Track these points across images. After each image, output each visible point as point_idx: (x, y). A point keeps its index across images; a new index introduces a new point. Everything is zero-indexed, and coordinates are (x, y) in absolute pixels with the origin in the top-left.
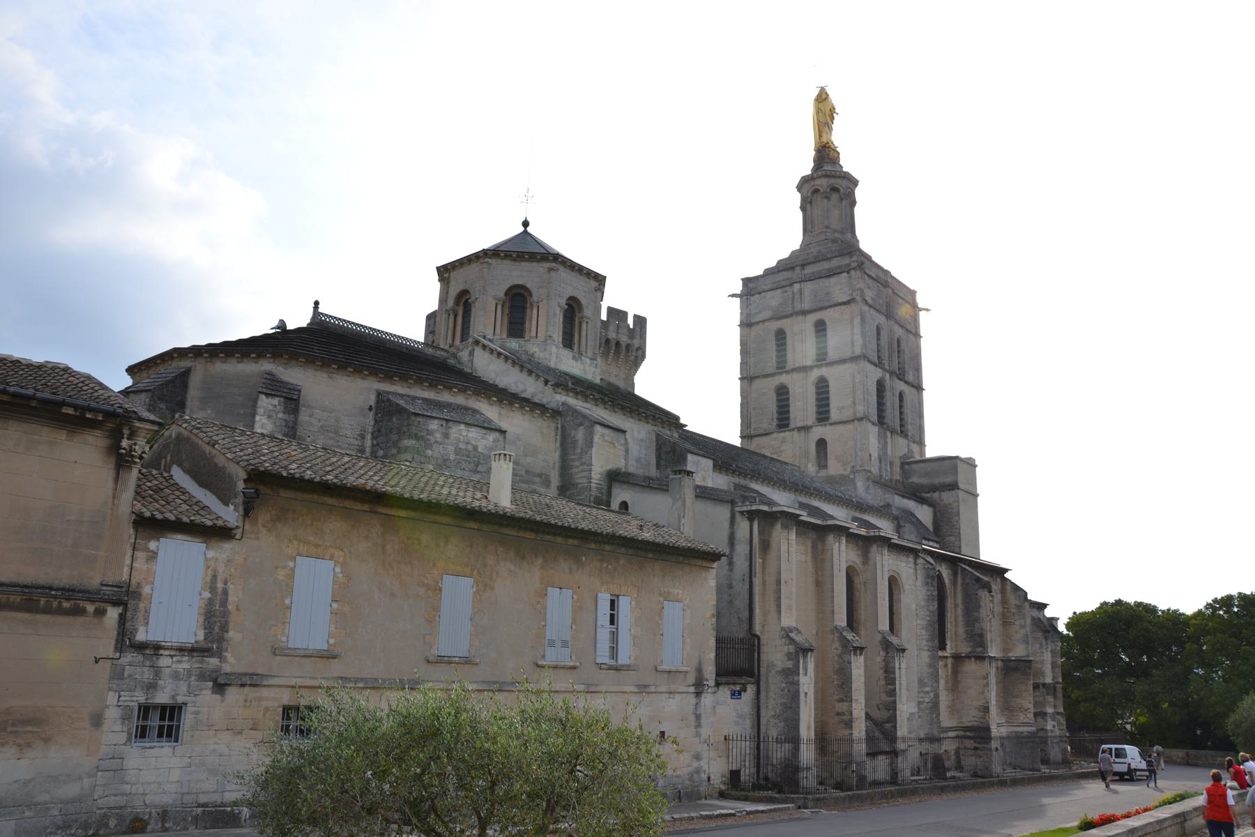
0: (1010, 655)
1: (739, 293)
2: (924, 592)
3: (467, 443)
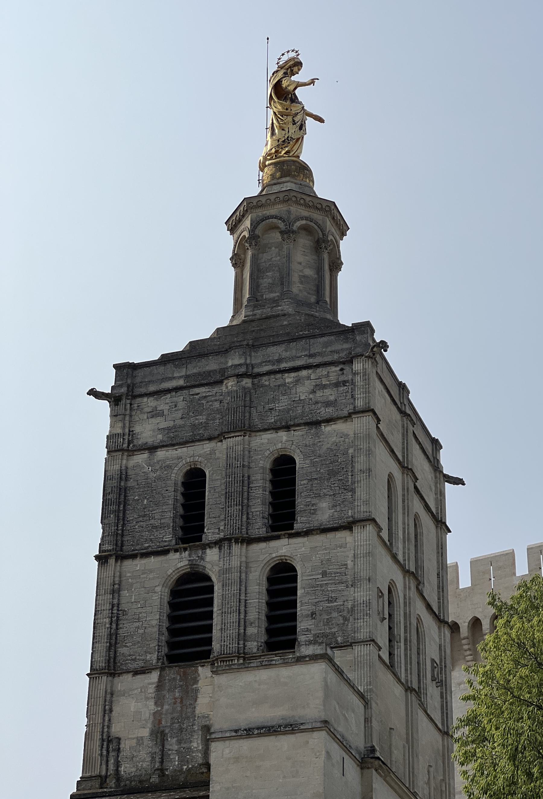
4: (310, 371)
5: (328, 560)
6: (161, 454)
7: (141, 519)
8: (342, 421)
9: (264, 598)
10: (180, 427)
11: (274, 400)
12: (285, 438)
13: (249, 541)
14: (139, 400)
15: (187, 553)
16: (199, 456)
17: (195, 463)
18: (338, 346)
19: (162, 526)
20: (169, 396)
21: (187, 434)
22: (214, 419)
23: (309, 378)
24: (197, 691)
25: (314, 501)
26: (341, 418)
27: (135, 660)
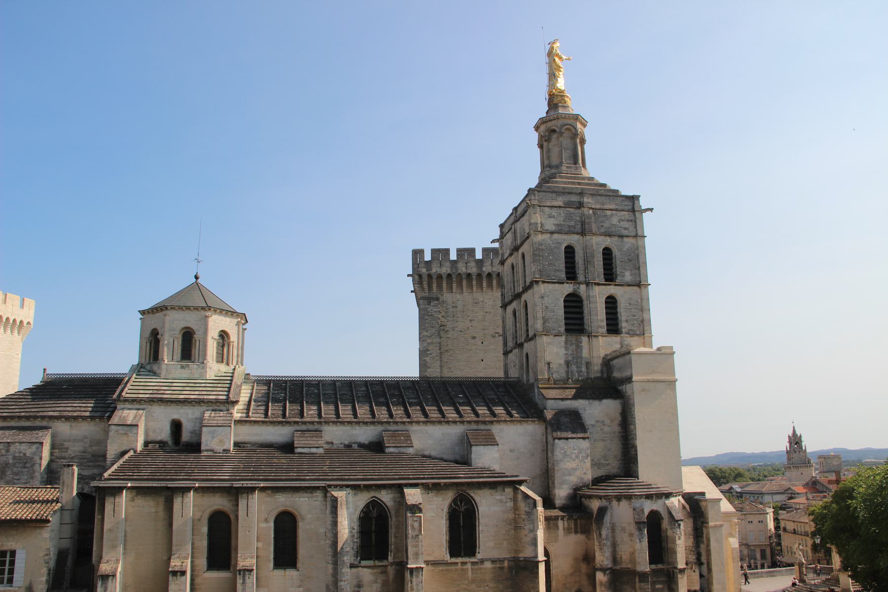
0: (521, 555)
2: (330, 519)
3: (20, 453)
4: (617, 212)
5: (631, 298)
6: (555, 236)
7: (549, 265)
8: (631, 238)
9: (604, 311)
10: (563, 225)
11: (603, 222)
12: (609, 240)
13: (599, 284)
14: (542, 208)
15: (572, 285)
17: (571, 243)
18: (626, 203)
19: (560, 271)
20: (556, 209)
21: (566, 229)
22: (577, 225)
24: (582, 347)
26: (632, 236)
27: (554, 329)
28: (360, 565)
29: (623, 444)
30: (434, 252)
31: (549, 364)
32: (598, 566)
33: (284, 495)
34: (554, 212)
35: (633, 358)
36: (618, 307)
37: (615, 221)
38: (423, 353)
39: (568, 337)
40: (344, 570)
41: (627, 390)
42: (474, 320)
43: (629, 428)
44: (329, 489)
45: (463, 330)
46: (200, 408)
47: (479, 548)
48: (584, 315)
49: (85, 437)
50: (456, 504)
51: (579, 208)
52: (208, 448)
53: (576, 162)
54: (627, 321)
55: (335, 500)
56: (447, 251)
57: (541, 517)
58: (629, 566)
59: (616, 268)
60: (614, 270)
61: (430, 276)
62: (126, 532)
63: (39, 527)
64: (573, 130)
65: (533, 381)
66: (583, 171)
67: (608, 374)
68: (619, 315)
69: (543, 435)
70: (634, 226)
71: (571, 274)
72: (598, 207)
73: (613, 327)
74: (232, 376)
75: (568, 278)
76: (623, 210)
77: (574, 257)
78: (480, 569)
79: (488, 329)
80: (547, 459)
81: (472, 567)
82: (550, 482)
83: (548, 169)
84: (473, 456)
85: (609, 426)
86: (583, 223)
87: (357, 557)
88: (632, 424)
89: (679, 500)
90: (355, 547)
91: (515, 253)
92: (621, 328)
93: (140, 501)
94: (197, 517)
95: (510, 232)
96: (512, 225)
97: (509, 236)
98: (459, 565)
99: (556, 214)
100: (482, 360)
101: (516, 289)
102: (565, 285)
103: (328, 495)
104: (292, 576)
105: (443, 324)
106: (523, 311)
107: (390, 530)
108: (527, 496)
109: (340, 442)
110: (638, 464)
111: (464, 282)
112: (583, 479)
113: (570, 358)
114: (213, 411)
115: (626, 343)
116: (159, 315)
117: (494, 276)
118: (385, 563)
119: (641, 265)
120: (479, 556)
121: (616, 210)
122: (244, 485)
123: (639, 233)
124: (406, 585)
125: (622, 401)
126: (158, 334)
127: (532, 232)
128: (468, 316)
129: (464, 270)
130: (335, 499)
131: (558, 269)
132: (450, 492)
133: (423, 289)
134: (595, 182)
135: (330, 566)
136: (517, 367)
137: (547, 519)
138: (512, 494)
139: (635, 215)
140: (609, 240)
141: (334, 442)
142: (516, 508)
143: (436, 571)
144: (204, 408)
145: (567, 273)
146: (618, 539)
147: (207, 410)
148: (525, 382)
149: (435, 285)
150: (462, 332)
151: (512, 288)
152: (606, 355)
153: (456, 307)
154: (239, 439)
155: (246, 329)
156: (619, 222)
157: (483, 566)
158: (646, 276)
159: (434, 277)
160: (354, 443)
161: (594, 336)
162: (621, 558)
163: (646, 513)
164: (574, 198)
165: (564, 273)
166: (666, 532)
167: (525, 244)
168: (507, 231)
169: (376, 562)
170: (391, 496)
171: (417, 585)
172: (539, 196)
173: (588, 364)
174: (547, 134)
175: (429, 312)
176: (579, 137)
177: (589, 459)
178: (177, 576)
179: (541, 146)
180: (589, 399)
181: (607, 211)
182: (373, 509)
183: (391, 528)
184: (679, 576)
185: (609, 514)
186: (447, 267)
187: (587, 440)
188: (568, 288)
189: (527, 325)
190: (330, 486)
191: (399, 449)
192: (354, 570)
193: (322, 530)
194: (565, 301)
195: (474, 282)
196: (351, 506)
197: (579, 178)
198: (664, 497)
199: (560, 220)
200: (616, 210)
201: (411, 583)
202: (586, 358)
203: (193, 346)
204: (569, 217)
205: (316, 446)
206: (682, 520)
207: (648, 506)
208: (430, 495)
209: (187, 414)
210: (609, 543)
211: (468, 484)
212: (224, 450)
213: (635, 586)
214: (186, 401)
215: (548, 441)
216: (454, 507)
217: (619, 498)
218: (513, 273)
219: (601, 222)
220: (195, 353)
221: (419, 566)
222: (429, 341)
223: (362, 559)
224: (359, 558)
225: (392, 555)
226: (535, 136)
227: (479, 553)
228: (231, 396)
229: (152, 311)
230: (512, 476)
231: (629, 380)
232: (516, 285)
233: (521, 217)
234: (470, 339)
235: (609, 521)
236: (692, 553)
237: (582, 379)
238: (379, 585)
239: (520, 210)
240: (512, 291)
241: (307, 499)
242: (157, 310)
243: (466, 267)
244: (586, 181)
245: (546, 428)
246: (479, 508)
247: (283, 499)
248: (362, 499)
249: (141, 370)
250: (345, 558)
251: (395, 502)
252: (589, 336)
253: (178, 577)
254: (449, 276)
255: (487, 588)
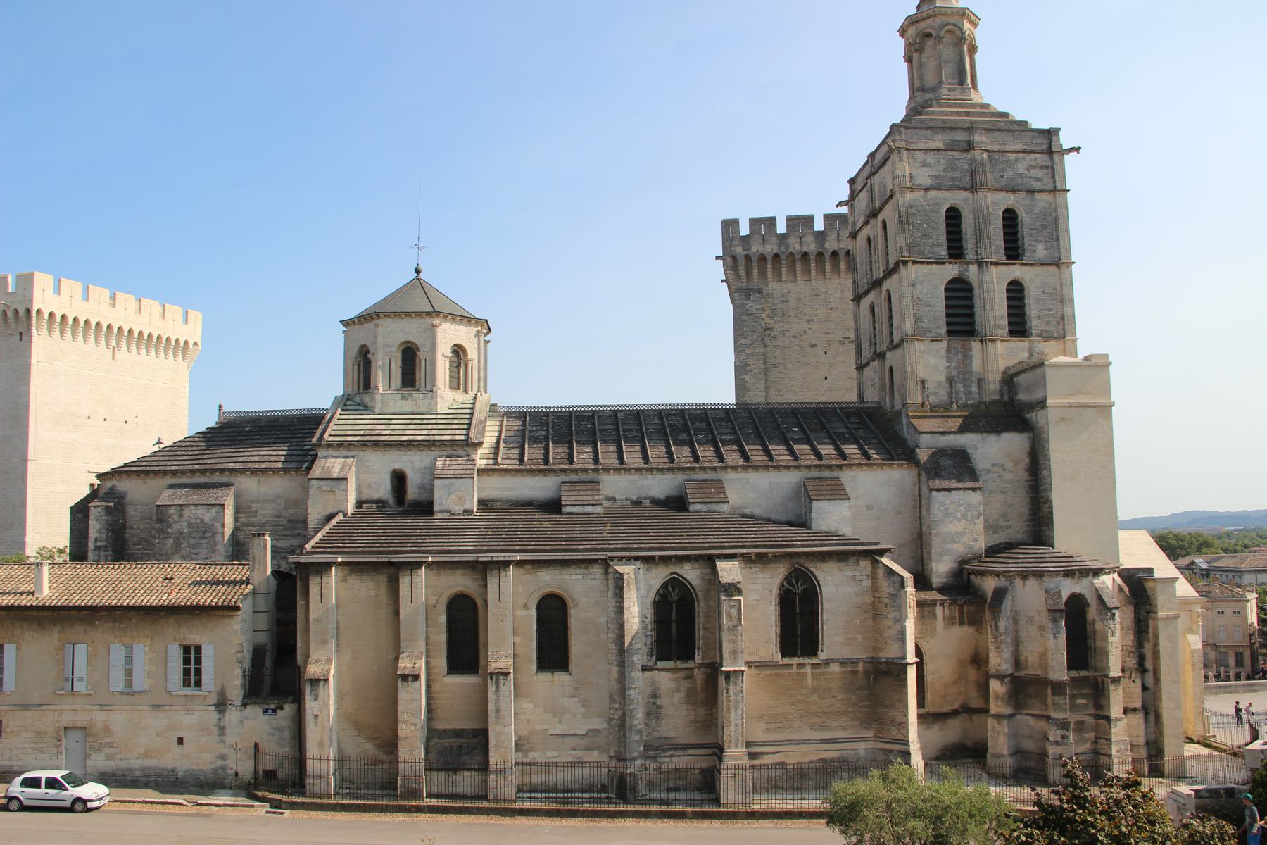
0: (881, 655)
1: (847, 199)
2: (614, 604)
5: (1045, 284)
6: (932, 194)
9: (1005, 303)
13: (996, 264)
14: (912, 152)
16: (959, 200)
19: (939, 245)
20: (932, 153)
23: (1024, 159)
24: (971, 356)
25: (1034, 243)
26: (1047, 191)
28: (655, 667)
29: (1032, 498)
30: (754, 222)
31: (923, 382)
32: (992, 671)
33: (550, 572)
34: (930, 158)
35: (1049, 371)
36: (1026, 298)
37: (1021, 168)
38: (741, 369)
39: (951, 342)
40: (633, 674)
41: (1039, 419)
42: (813, 320)
43: (1040, 474)
44: (610, 563)
45: (797, 335)
46: (429, 453)
47: (823, 644)
48: (976, 309)
49: (278, 497)
50: (790, 583)
51: (967, 151)
52: (443, 508)
53: (962, 82)
54: (1039, 317)
55: (620, 578)
56: (772, 221)
57: (912, 601)
58: (1038, 673)
59: (1023, 239)
60: (1020, 243)
61: (748, 258)
62: (338, 622)
63: (223, 616)
64: (958, 33)
65: (901, 407)
66: (973, 95)
67: (1009, 397)
68: (1027, 309)
69: (914, 485)
70: (1050, 176)
71: (956, 250)
72: (996, 147)
73: (1018, 327)
74: (472, 408)
75: (951, 256)
76: (1034, 152)
77: (959, 225)
78: (824, 674)
79: (833, 333)
80: (920, 518)
81: (813, 671)
82: (925, 552)
83: (920, 93)
84: (814, 515)
85: (1011, 472)
86: (973, 174)
87: (652, 656)
88: (1045, 469)
89: (1113, 579)
90: (648, 643)
91: (873, 221)
92: (1031, 327)
93: (355, 581)
94: (433, 602)
95: (865, 190)
96: (867, 179)
97: (863, 196)
98: (795, 667)
99: (932, 161)
100: (826, 378)
101: (874, 273)
102: (947, 265)
103: (610, 570)
104: (562, 682)
105: (768, 326)
106: (884, 305)
107: (697, 619)
108: (891, 572)
109: (625, 497)
110: (1053, 526)
111: (799, 266)
112: (972, 547)
113: (954, 373)
114: (448, 456)
115: (1037, 350)
116: (369, 326)
117: (842, 256)
118: (690, 664)
119: (1062, 233)
120: (822, 656)
121: (1024, 152)
122: (495, 559)
123: (1059, 186)
124: (720, 695)
125: (1030, 435)
126: (368, 352)
127: (897, 188)
128: (805, 315)
129: (798, 247)
130: (619, 576)
131: (935, 242)
132: (781, 565)
133: (739, 277)
134: (991, 110)
135: (615, 669)
136: (877, 387)
137: (920, 604)
138: (870, 569)
139: (1052, 159)
140: (1013, 198)
141: (617, 498)
142: (875, 589)
143: (761, 676)
144: (435, 453)
145: (949, 248)
146: (1023, 634)
147: (440, 456)
148: (889, 409)
149: (755, 271)
150: (796, 337)
151: (869, 272)
152: (1008, 368)
153: (787, 302)
154: (485, 495)
155: (489, 342)
156: (1028, 170)
157: (828, 670)
158: (1069, 251)
159: (755, 259)
160: (645, 499)
161: (990, 340)
162: (1026, 661)
163: (1065, 596)
164: (960, 136)
165: (945, 248)
166: (1094, 624)
167: (887, 206)
168: (860, 188)
169: (678, 662)
170: (698, 572)
171: (735, 695)
172: (906, 134)
173: (980, 382)
174: (918, 40)
175: (747, 310)
176: (967, 42)
177: (982, 518)
178: (408, 682)
179: (909, 59)
180: (981, 432)
181: (1010, 154)
182: (673, 590)
183: (699, 616)
184: (1112, 687)
185: (1010, 597)
186: (773, 244)
187: (979, 492)
188: (951, 270)
189: (891, 325)
190: (612, 558)
191: (709, 505)
192: (647, 674)
193: (603, 620)
194: (946, 290)
195: (813, 265)
196: (642, 586)
197: (967, 106)
198: (1091, 574)
199: (938, 170)
200: (1024, 152)
201: (727, 692)
202: (979, 373)
203: (417, 368)
204: (952, 165)
205: (591, 502)
206: (1117, 608)
207: (1068, 588)
208: (753, 569)
209: (413, 462)
210: (1009, 640)
211: (807, 555)
212: (465, 511)
213: (1046, 701)
214: (410, 445)
215: (922, 493)
216: (787, 586)
217: (1024, 576)
218: (870, 250)
219: (1000, 171)
220: (420, 378)
221: (737, 669)
222: (749, 351)
223: (659, 659)
224: (654, 658)
225: (701, 653)
226: (900, 45)
227: (822, 651)
228: (472, 435)
229: (359, 321)
230: (869, 544)
231: (1042, 404)
232: (874, 267)
233: (880, 168)
234: (808, 347)
235: (1009, 608)
236: (1131, 655)
237: (972, 405)
238: (683, 695)
239: (878, 158)
240: (869, 276)
241: (580, 577)
242: (365, 319)
243: (801, 243)
244: (978, 110)
245: (919, 475)
246: (823, 589)
247: (547, 577)
248: (659, 576)
249: (348, 403)
250: (635, 658)
251: (703, 579)
252: (981, 341)
253: (410, 683)
254: (776, 256)
255: (833, 700)
